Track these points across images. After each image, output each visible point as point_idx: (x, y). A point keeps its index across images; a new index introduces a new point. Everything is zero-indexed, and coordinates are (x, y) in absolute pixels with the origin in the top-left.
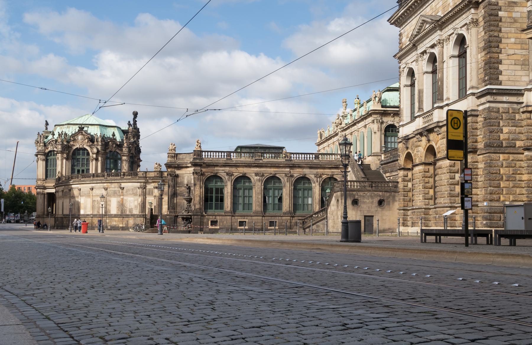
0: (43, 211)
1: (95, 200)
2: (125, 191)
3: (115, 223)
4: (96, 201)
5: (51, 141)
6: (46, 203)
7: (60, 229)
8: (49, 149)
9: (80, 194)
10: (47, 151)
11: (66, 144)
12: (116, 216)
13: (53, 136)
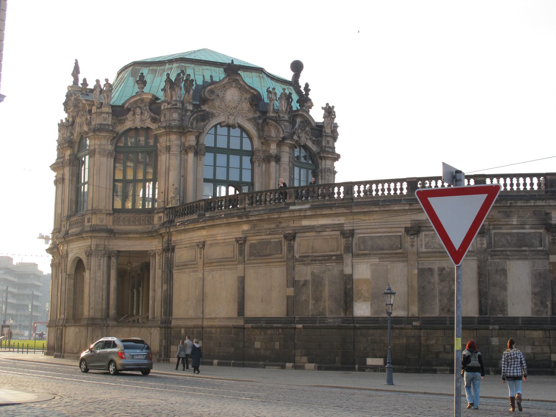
0: (104, 306)
1: (431, 270)
5: (136, 102)
7: (235, 365)
8: (128, 125)
10: (121, 129)
13: (143, 88)
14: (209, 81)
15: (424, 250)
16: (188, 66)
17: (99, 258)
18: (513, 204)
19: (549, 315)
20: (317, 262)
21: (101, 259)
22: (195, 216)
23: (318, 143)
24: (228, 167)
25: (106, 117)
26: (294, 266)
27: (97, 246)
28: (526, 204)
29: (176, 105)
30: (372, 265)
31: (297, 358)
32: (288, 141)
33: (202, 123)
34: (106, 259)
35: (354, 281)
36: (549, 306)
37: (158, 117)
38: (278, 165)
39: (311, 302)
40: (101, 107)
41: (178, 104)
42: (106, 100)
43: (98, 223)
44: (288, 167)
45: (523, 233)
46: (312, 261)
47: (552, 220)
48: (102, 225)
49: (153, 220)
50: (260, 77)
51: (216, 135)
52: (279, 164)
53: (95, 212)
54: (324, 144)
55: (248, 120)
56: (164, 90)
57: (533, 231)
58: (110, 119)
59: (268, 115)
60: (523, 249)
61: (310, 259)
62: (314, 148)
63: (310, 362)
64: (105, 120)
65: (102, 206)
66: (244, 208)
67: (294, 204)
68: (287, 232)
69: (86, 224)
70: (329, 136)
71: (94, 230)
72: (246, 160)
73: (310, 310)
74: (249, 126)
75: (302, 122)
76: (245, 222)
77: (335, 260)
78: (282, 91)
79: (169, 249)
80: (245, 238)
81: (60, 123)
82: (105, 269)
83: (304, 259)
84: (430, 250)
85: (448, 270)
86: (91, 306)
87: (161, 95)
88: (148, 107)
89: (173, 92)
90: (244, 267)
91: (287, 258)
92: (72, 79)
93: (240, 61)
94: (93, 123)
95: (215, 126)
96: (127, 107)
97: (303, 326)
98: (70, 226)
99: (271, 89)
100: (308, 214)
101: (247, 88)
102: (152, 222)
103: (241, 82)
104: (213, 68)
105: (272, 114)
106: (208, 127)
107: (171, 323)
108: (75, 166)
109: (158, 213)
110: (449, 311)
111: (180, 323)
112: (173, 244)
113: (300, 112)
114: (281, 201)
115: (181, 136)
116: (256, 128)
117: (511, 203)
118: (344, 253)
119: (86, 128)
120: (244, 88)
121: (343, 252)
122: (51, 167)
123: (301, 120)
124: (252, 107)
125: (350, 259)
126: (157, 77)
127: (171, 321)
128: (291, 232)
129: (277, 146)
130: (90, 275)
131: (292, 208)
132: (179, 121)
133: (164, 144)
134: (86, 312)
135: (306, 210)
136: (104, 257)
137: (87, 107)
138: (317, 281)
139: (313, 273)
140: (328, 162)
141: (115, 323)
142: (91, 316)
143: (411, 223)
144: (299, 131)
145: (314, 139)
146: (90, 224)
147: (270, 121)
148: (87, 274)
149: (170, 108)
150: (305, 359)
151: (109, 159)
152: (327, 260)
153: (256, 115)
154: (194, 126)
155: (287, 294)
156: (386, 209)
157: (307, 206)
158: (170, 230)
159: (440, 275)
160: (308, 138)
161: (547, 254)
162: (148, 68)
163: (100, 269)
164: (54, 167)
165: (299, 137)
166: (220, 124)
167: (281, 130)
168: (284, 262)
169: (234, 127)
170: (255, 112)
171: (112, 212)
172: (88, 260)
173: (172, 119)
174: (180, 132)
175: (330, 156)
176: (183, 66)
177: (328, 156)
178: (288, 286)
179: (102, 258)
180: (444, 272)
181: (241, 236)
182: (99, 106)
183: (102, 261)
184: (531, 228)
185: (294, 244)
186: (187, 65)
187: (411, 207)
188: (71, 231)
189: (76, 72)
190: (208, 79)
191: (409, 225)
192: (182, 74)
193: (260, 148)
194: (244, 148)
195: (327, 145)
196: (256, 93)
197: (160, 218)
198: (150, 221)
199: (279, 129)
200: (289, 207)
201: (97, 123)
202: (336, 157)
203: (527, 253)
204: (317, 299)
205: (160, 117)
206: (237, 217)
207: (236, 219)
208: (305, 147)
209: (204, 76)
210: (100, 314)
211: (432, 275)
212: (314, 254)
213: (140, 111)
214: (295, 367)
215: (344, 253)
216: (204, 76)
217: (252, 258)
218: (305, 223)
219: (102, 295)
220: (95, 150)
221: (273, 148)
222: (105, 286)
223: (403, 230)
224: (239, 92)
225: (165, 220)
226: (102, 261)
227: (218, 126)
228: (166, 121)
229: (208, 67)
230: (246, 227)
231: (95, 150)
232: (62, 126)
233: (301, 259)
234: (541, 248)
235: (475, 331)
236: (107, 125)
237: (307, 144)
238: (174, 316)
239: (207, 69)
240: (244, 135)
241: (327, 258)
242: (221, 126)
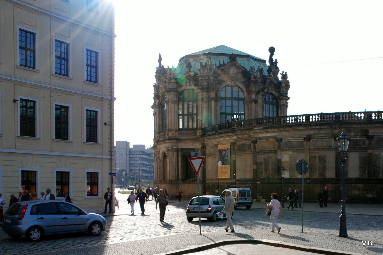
0: (176, 175)
2: (374, 142)
3: (357, 192)
4: (317, 158)
6: (180, 164)
9: (279, 147)
11: (213, 79)
12: (357, 180)
13: (190, 69)
14: (222, 64)
15: (312, 148)
16: (212, 57)
17: (173, 152)
18: (351, 127)
19: (367, 176)
20: (266, 154)
21: (174, 153)
22: (214, 132)
23: (278, 92)
24: (232, 107)
25: (173, 85)
26: (256, 155)
27: (172, 146)
28: (357, 126)
29: (205, 78)
30: (289, 155)
31: (258, 197)
32: (261, 93)
33: (219, 86)
34: (176, 153)
35: (282, 162)
36: (367, 173)
37: (197, 84)
38: (256, 105)
39: (264, 171)
40: (170, 80)
41: (206, 77)
42: (173, 76)
43: (172, 135)
44: (261, 106)
45: (356, 140)
46: (264, 153)
47: (369, 133)
48: (174, 137)
49: (197, 134)
50: (248, 60)
51: (226, 91)
52: (257, 104)
53: (170, 130)
54: (281, 92)
55: (241, 83)
56: (199, 70)
57: (361, 138)
58: (175, 85)
59: (251, 80)
60: (356, 147)
61: (263, 152)
62: (276, 94)
63: (263, 198)
64: (172, 86)
65: (173, 127)
66: (235, 129)
67: (256, 127)
68: (253, 140)
69: (166, 136)
70: (284, 88)
71: (170, 139)
72: (241, 103)
73: (263, 176)
74: (242, 86)
75: (269, 82)
76: (235, 135)
77: (274, 152)
78: (258, 67)
79: (204, 147)
80: (235, 142)
81: (154, 85)
82: (176, 157)
83: (260, 152)
84: (314, 148)
85: (323, 157)
86: (170, 174)
87: (198, 72)
88: (193, 79)
89: (204, 71)
90: (235, 156)
91: (253, 152)
92: (158, 64)
93: (238, 52)
94: (167, 88)
95: (225, 87)
96: (183, 79)
97: (260, 183)
98: (160, 137)
99: (252, 67)
100: (261, 131)
101: (240, 67)
102: (196, 134)
103: (237, 64)
104: (224, 57)
105: (253, 79)
106: (222, 87)
107: (205, 182)
108: (161, 108)
109: (199, 130)
110: (323, 175)
111: (210, 182)
112: (205, 145)
113: (268, 77)
114: (251, 125)
115: (208, 93)
116: (245, 87)
117: (351, 126)
118: (278, 149)
119: (164, 90)
120: (238, 67)
121: (277, 149)
122: (151, 107)
123: (269, 81)
124: (243, 76)
125: (280, 152)
126: (197, 63)
127: (206, 181)
128: (254, 140)
129: (255, 95)
130: (169, 160)
131: (255, 128)
132: (207, 85)
133: (200, 97)
134: (168, 177)
135: (260, 129)
136: (175, 152)
137: (164, 79)
138: (266, 162)
139: (264, 159)
140: (284, 101)
141: (182, 182)
142: (170, 179)
143: (306, 135)
144: (268, 86)
145: (276, 90)
146: (168, 136)
147: (252, 83)
148: (168, 160)
149: (202, 79)
150: (261, 197)
151: (175, 105)
152: (270, 152)
153: (245, 80)
154: (214, 88)
155: (254, 168)
156: (295, 129)
157: (261, 128)
158: (203, 139)
159: (319, 159)
160: (273, 89)
161: (367, 149)
162: (193, 58)
163: (174, 157)
164: (152, 107)
165: (268, 89)
166: (227, 85)
167: (257, 87)
168: (252, 153)
169: (234, 87)
170: (245, 79)
171: (178, 130)
172: (168, 153)
173: (204, 84)
174: (208, 91)
175: (284, 98)
176: (209, 57)
177: (283, 98)
178: (254, 165)
179: (174, 152)
180: (321, 158)
181: (233, 141)
182: (169, 79)
183: (174, 153)
184: (359, 137)
185: (256, 145)
186: (211, 56)
187: (307, 128)
188: (160, 140)
189: (160, 59)
190: (222, 63)
191: (306, 137)
192: (208, 62)
193: (248, 97)
194: (240, 97)
195: (283, 93)
196: (244, 69)
197: (200, 132)
198: (196, 134)
199: (256, 87)
200: (253, 128)
201: (169, 88)
202: (287, 98)
203: (358, 149)
204: (266, 170)
205: (198, 84)
206: (231, 133)
207: (231, 134)
208: (272, 94)
209: (220, 61)
210: (175, 178)
211: (316, 159)
212: (265, 150)
213: (189, 81)
214: (257, 201)
215: (278, 149)
216: (220, 61)
217: (238, 151)
218: (261, 135)
219: (175, 170)
220: (168, 101)
221: (253, 96)
222: (176, 165)
223: (303, 138)
224: (236, 69)
225: (202, 134)
226: (174, 153)
227: (227, 87)
228: (201, 86)
229: (222, 57)
230: (235, 137)
231: (168, 101)
232: (155, 86)
233: (259, 152)
234: (364, 147)
235: (334, 184)
236: (174, 88)
237: (273, 92)
238: (207, 178)
239: (222, 58)
240: (240, 90)
241: (270, 152)
242: (228, 87)
